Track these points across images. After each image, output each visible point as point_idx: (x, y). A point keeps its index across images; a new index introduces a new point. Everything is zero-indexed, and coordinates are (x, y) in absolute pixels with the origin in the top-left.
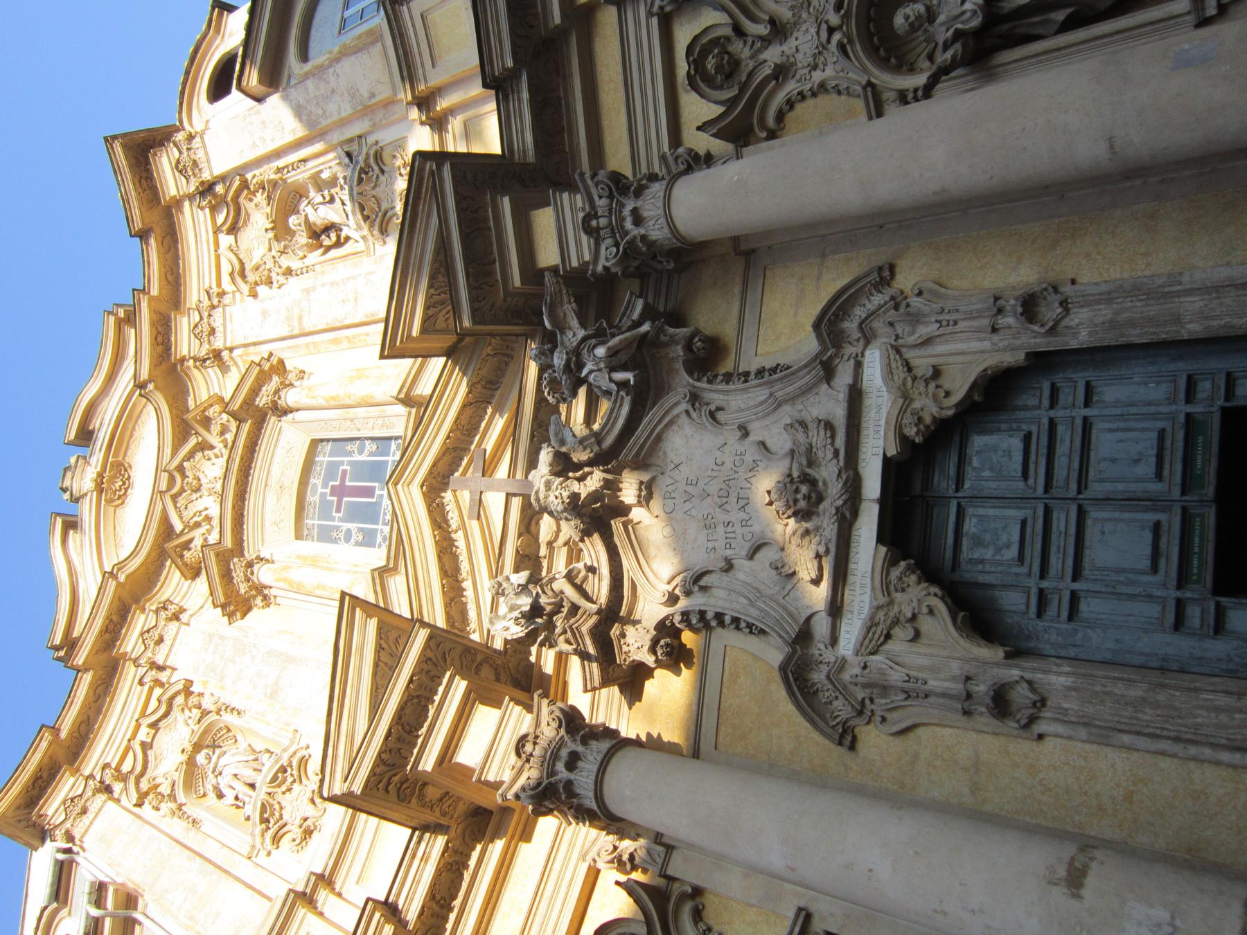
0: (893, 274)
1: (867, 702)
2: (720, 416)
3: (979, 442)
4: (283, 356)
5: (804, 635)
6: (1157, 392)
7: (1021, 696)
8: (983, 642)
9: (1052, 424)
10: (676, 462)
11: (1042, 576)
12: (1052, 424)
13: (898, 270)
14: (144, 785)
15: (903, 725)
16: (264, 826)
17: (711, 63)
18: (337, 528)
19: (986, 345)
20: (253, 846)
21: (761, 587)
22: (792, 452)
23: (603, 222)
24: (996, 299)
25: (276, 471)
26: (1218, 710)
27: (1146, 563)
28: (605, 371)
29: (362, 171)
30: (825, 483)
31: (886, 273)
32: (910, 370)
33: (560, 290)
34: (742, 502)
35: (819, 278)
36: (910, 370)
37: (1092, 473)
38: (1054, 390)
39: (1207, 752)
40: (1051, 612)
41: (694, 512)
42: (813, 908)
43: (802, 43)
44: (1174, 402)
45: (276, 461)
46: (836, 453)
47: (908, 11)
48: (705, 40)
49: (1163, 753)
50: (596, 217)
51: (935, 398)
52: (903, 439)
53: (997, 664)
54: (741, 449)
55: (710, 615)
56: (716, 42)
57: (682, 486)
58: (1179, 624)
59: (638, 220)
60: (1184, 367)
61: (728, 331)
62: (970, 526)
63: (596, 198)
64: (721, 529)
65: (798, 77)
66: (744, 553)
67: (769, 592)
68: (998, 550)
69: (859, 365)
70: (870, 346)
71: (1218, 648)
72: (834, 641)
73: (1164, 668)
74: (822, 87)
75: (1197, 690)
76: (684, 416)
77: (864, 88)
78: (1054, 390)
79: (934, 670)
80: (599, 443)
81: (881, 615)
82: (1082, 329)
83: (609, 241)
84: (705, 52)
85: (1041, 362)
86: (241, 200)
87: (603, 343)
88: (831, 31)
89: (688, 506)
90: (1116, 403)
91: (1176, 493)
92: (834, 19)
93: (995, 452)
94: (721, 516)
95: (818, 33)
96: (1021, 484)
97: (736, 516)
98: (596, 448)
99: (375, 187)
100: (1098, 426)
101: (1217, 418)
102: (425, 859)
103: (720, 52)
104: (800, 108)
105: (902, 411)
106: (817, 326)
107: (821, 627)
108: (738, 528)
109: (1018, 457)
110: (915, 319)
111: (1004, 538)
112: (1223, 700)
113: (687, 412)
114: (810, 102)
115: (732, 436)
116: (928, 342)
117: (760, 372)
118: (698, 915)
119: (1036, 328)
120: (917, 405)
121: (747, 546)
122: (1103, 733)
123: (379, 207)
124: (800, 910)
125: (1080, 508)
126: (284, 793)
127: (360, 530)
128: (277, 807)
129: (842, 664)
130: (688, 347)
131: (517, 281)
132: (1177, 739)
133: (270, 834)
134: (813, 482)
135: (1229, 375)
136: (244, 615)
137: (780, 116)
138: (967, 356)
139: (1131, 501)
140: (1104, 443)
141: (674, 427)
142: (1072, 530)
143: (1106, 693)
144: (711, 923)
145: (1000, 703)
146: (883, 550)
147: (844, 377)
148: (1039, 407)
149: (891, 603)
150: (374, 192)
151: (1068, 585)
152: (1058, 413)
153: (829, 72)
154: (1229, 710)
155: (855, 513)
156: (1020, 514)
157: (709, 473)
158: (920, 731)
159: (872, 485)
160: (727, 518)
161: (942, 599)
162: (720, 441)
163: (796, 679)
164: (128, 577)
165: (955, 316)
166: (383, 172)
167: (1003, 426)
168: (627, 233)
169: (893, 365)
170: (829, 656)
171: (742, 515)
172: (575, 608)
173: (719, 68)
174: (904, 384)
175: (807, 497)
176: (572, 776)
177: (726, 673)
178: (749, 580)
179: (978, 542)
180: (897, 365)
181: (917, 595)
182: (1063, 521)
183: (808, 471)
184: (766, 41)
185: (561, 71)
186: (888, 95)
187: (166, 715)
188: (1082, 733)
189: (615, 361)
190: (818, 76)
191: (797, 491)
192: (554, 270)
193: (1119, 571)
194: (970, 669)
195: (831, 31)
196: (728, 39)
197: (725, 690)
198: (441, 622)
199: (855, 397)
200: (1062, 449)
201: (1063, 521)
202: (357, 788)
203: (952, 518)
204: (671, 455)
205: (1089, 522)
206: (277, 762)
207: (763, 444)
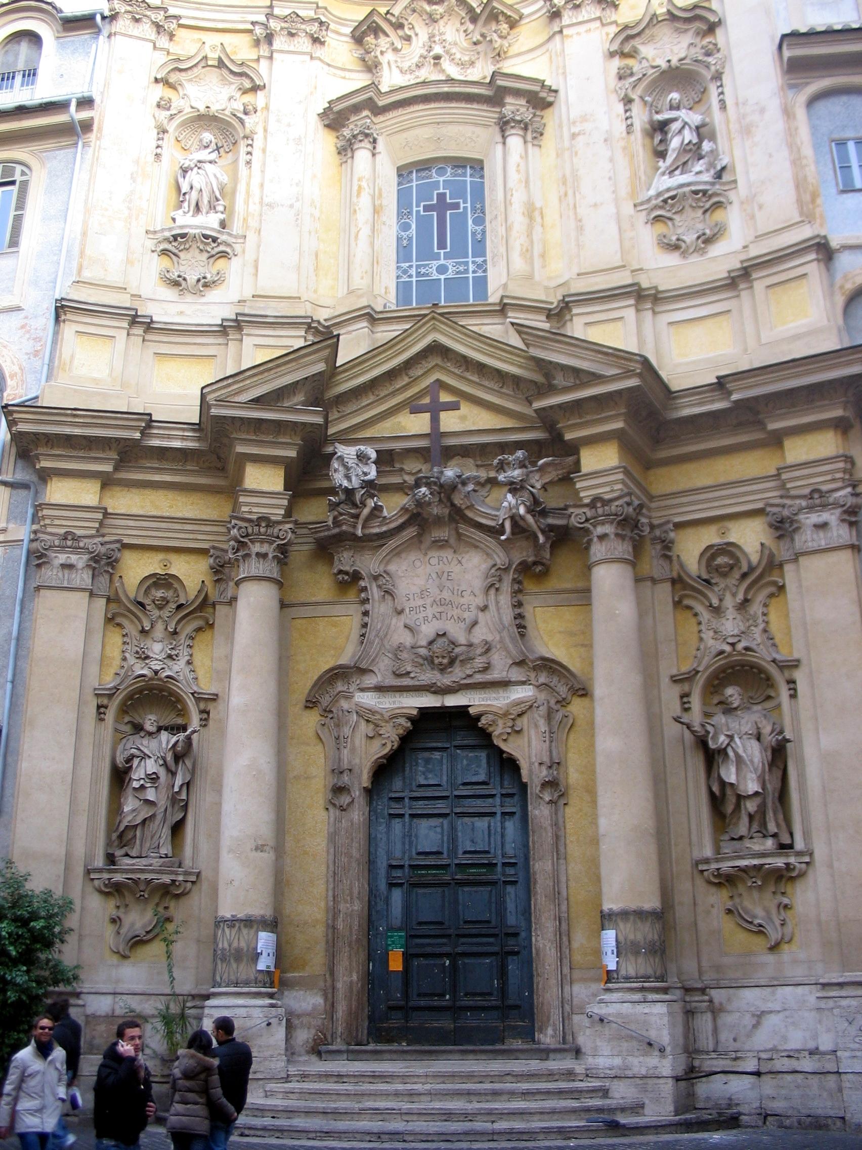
0: (582, 695)
1: (331, 716)
2: (492, 591)
3: (483, 755)
4: (556, 105)
5: (363, 671)
6: (510, 849)
7: (345, 800)
8: (371, 774)
9: (493, 796)
10: (463, 561)
11: (410, 798)
12: (493, 796)
13: (583, 699)
14: (173, 78)
15: (322, 736)
16: (172, 239)
17: (721, 560)
18: (410, 213)
19: (534, 759)
20: (155, 232)
21: (388, 637)
22: (470, 645)
23: (600, 511)
24: (558, 763)
25: (452, 130)
26: (351, 889)
28: (510, 514)
29: (705, 192)
30: (451, 672)
31: (580, 693)
32: (519, 715)
33: (563, 469)
34: (438, 615)
35: (583, 645)
36: (519, 715)
37: (466, 819)
38: (511, 795)
39: (331, 886)
40: (394, 805)
41: (431, 581)
42: (220, 701)
43: (731, 624)
44: (503, 857)
45: (461, 128)
46: (469, 676)
47: (736, 696)
48: (738, 554)
49: (328, 867)
50: (603, 506)
51: (501, 734)
52: (478, 718)
53: (360, 784)
54: (472, 608)
55: (368, 607)
56: (738, 560)
57: (447, 569)
58: (392, 867)
59: (602, 537)
60: (520, 861)
61: (554, 583)
62: (437, 755)
63: (616, 503)
64: (420, 602)
65: (712, 619)
66: (408, 622)
67: (386, 643)
68: (424, 773)
69: (523, 683)
70: (535, 689)
71: (383, 885)
72: (362, 690)
73: (371, 863)
74: (701, 639)
75: (359, 879)
76: (491, 563)
77: (694, 669)
78: (511, 795)
79: (353, 750)
80: (468, 508)
81: (378, 717)
82: (540, 812)
83: (589, 514)
84: (732, 555)
85: (524, 787)
86: (698, 25)
87: (529, 511)
88: (733, 645)
89: (434, 576)
90: (503, 828)
91: (457, 862)
92: (740, 646)
93: (476, 767)
94: (429, 601)
95: (733, 636)
96: (460, 782)
97: (430, 612)
98: (463, 507)
99: (691, 206)
100: (492, 820)
101: (495, 877)
102: (184, 438)
103: (730, 565)
104: (693, 621)
105: (495, 714)
106: (543, 659)
107: (370, 681)
108: (423, 614)
109: (474, 779)
110: (549, 717)
111: (430, 776)
112: (356, 891)
113: (495, 565)
114: (695, 629)
115: (480, 601)
116: (536, 726)
117: (520, 616)
118: (199, 630)
119: (539, 788)
120: (500, 722)
121: (411, 623)
122: (332, 838)
123: (675, 213)
124: (217, 695)
125: (448, 814)
126: (198, 247)
127: (410, 239)
128: (187, 246)
129: (349, 698)
130: (535, 563)
131: (568, 436)
132: (335, 873)
133: (166, 246)
134: (452, 662)
135: (516, 882)
136: (327, 126)
137: (689, 608)
138: (528, 749)
139: (453, 840)
140: (481, 824)
141: (485, 556)
142: (436, 812)
143: (352, 839)
144: (197, 639)
145: (339, 790)
146: (415, 712)
147: (516, 674)
148: (502, 788)
149: (387, 722)
150: (687, 207)
152: (498, 800)
153: (711, 642)
154: (351, 894)
155: (435, 693)
156: (444, 783)
157: (456, 588)
158: (319, 747)
159: (452, 701)
160: (428, 606)
161: (392, 749)
162: (477, 592)
163: (336, 674)
165: (548, 742)
166: (705, 212)
167: (492, 769)
168: (595, 526)
169: (523, 705)
170: (353, 688)
171: (430, 616)
172: (357, 516)
173: (719, 566)
174: (510, 714)
175: (441, 664)
176: (254, 556)
177: (337, 618)
178: (392, 626)
179: (427, 761)
180: (523, 707)
181: (391, 737)
182: (441, 807)
183: (458, 662)
184: (734, 595)
185: (740, 426)
186: (686, 687)
187: (232, 72)
188: (332, 830)
189: (517, 518)
190: (708, 635)
191: (443, 657)
192: (578, 463)
193: (416, 836)
194: (356, 770)
195: (733, 645)
196: (740, 568)
197: (326, 619)
198: (331, 431)
199: (505, 684)
200: (479, 802)
201: (441, 807)
202: (214, 411)
203: (440, 745)
204: (467, 557)
205: (441, 820)
206: (219, 232)
207: (475, 623)
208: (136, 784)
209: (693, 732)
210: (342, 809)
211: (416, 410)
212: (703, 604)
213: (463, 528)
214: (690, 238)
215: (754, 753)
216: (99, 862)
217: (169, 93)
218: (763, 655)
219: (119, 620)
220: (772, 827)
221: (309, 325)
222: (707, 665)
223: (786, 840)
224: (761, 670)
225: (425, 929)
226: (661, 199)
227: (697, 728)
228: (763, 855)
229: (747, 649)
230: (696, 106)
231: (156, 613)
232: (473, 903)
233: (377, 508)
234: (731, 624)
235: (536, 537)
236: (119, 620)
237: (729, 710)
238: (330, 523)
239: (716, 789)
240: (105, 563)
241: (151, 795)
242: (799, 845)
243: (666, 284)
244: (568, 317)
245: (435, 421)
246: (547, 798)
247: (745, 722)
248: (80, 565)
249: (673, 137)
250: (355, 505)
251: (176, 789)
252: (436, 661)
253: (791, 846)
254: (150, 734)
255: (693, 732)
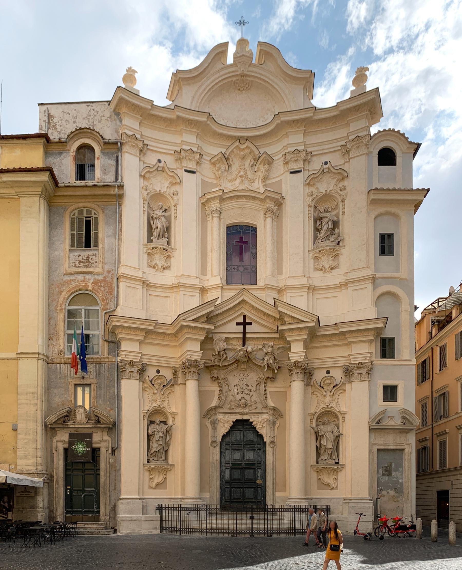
7: (214, 444)
27: (234, 458)
71: (224, 469)
88: (328, 406)
106: (273, 407)
146: (235, 420)
151: (231, 448)
159: (245, 417)
164: (209, 125)
170: (217, 412)
172: (220, 360)
208: (156, 439)
209: (314, 430)
210: (214, 447)
211: (238, 324)
212: (320, 393)
213: (251, 365)
214: (327, 266)
215: (331, 437)
216: (146, 462)
217: (146, 183)
218: (336, 410)
219: (146, 389)
220: (334, 458)
221: (201, 288)
222: (319, 410)
223: (337, 461)
224: (334, 413)
225: (235, 481)
226: (319, 250)
227: (316, 429)
228: (331, 465)
229: (331, 407)
230: (332, 211)
231: (157, 387)
232: (249, 474)
233: (226, 357)
234: (328, 399)
235: (274, 370)
236: (146, 389)
237: (324, 424)
238: (213, 361)
239: (318, 446)
240: (142, 371)
241: (161, 442)
242: (341, 463)
243: (318, 283)
244: (285, 293)
245: (244, 329)
246: (272, 446)
247: (328, 428)
248: (135, 371)
249: (325, 225)
250: (220, 356)
251: (167, 441)
252: (242, 405)
253: (338, 463)
254: (158, 424)
255: (314, 430)
